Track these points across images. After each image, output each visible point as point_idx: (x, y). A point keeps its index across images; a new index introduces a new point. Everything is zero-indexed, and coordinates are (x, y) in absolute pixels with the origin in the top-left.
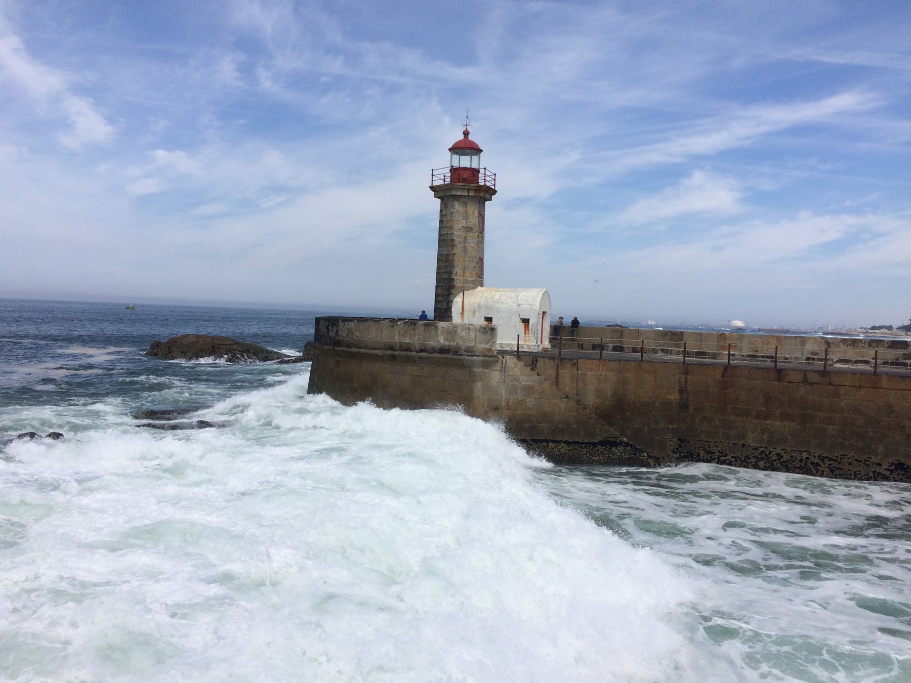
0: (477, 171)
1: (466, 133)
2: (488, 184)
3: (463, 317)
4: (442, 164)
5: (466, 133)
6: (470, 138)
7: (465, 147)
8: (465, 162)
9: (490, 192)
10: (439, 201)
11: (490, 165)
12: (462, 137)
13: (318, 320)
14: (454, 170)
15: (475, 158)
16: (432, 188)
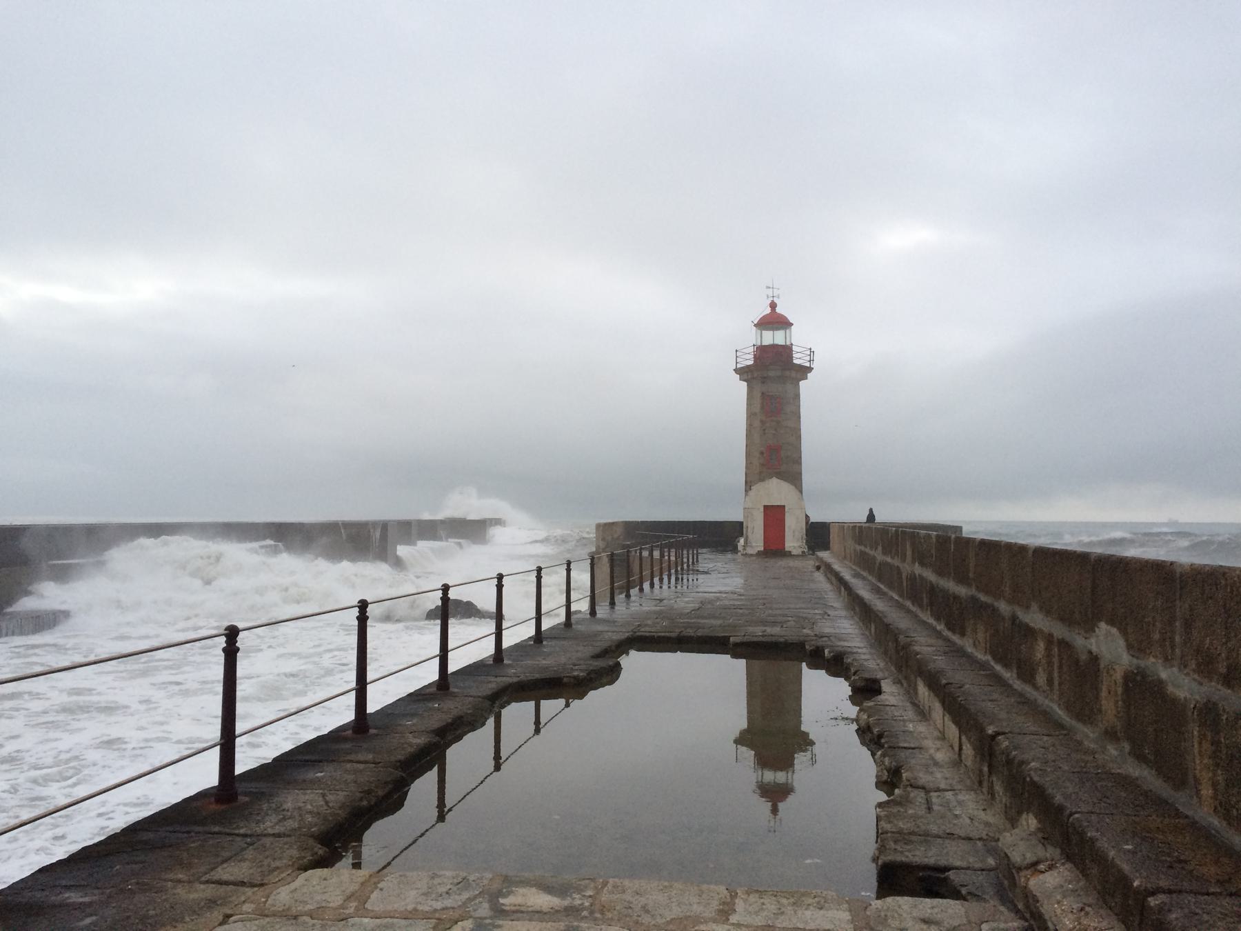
1: (773, 306)
5: (773, 306)
6: (778, 310)
7: (774, 321)
9: (804, 371)
10: (744, 385)
12: (768, 310)
16: (736, 371)
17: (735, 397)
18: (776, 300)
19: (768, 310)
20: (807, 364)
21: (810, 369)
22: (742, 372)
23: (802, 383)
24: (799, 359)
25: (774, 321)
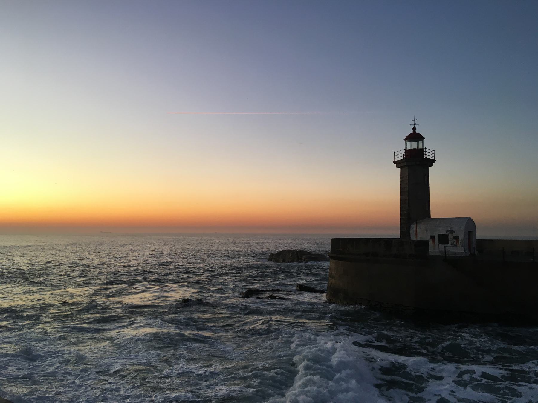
0: (422, 150)
1: (414, 129)
2: (428, 157)
3: (416, 236)
4: (400, 148)
5: (414, 129)
6: (417, 131)
7: (415, 137)
8: (414, 145)
9: (431, 162)
10: (399, 169)
11: (430, 146)
13: (333, 240)
14: (407, 151)
15: (420, 143)
16: (395, 162)
17: (395, 176)
18: (416, 126)
19: (412, 132)
20: (433, 158)
21: (434, 161)
22: (398, 163)
23: (429, 168)
24: (429, 155)
25: (415, 137)
